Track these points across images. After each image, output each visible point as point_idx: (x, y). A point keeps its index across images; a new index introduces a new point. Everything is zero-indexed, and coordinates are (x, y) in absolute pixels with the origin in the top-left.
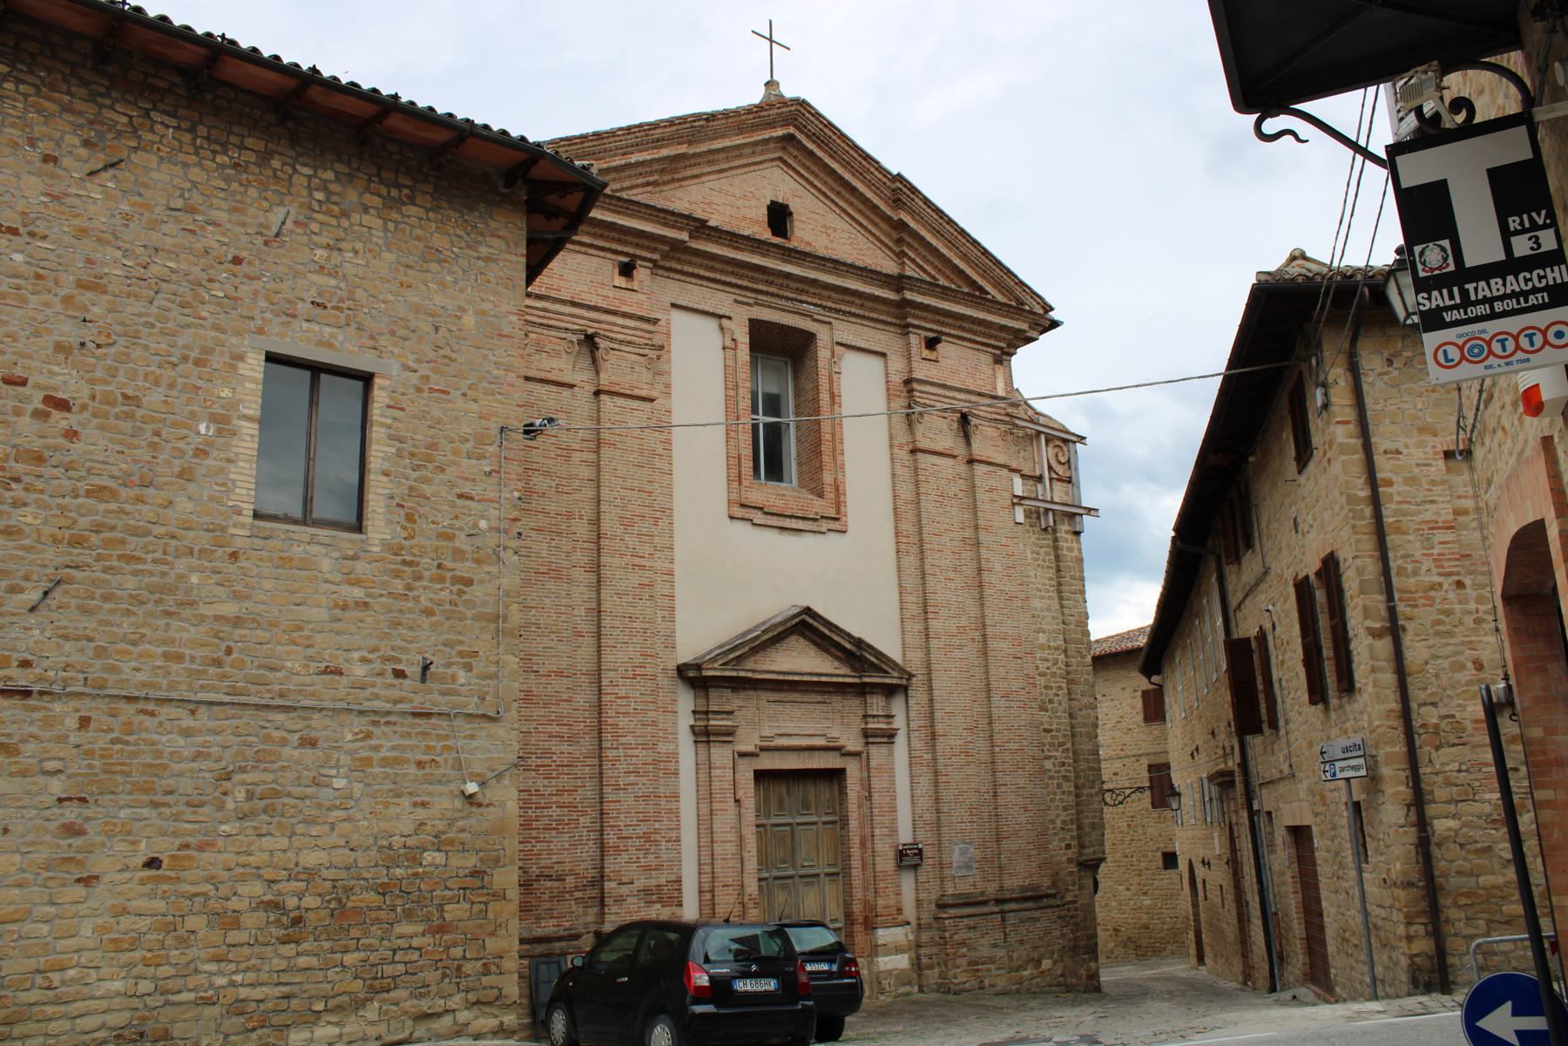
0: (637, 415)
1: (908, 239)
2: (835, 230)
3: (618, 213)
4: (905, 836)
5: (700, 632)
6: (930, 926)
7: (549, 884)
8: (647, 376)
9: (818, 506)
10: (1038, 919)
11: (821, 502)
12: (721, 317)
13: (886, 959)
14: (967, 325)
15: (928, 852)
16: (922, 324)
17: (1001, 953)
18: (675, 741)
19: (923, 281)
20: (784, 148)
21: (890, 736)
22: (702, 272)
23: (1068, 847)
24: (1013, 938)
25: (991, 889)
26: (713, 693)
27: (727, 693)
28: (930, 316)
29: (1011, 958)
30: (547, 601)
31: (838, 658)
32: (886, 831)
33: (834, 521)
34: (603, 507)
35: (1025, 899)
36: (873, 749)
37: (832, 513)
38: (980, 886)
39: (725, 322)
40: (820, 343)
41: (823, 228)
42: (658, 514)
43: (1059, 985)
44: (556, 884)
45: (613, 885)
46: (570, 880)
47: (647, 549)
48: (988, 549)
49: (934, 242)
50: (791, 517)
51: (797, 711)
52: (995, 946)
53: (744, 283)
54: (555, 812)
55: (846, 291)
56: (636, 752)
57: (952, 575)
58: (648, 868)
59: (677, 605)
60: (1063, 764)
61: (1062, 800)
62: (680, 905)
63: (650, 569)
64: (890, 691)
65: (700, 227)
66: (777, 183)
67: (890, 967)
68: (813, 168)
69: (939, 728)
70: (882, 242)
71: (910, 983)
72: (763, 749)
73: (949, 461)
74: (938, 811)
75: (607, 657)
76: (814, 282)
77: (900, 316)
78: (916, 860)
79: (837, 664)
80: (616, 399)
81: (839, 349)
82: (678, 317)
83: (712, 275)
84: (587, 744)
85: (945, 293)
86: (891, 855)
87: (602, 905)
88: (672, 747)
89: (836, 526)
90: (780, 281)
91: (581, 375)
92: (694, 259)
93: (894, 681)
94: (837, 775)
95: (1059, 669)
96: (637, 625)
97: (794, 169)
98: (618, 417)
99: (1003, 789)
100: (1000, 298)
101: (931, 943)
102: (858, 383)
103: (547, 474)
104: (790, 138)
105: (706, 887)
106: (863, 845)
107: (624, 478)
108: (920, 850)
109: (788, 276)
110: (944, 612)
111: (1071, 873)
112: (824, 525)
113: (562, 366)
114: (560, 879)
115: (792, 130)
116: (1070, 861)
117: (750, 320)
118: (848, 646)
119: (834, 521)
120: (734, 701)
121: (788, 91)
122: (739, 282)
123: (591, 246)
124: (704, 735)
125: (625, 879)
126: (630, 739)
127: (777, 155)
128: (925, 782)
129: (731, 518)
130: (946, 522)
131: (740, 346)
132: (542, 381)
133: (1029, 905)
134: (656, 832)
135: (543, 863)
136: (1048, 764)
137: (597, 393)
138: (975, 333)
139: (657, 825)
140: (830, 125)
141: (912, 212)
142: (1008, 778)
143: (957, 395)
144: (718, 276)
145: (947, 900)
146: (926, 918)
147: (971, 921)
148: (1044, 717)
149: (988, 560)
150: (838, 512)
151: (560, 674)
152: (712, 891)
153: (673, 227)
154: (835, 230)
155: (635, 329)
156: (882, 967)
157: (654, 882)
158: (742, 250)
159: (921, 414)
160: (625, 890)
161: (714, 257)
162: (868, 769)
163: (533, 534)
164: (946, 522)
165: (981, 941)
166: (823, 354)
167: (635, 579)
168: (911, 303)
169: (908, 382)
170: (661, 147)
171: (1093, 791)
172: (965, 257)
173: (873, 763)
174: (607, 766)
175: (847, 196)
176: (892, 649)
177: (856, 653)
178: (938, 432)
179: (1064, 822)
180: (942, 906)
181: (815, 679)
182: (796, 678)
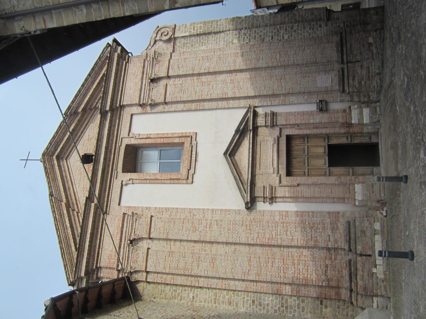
0: (157, 224)
1: (89, 106)
2: (89, 136)
3: (87, 232)
4: (313, 108)
5: (235, 201)
6: (352, 96)
7: (329, 271)
8: (143, 219)
9: (187, 145)
10: (351, 45)
11: (186, 144)
12: (122, 185)
13: (365, 120)
14: (118, 80)
15: (321, 98)
16: (119, 100)
17: (365, 64)
18: (275, 211)
19: (102, 103)
20: (62, 158)
21: (273, 114)
22: (107, 193)
23: (320, 26)
24: (358, 58)
25: (337, 66)
26: (257, 194)
27: (256, 188)
28: (115, 97)
29: (368, 58)
30: (223, 264)
31: (243, 138)
32: (311, 117)
33: (192, 137)
34: (190, 239)
35: (342, 50)
36: (278, 123)
37: (189, 139)
38: (336, 72)
39: (124, 183)
40: (129, 143)
41: (87, 144)
42: (192, 214)
43: (380, 34)
44: (329, 268)
45: (330, 244)
46: (328, 262)
47: (204, 222)
48: (201, 69)
49: (88, 96)
50: (191, 157)
51: (263, 157)
52: (362, 67)
53: (109, 176)
54: (301, 267)
55: (109, 134)
56: (279, 230)
57: (211, 86)
58: (324, 228)
59: (224, 208)
60: (286, 29)
61: (301, 30)
62: (338, 213)
63: (211, 220)
64: (255, 114)
65: (89, 199)
66: (74, 161)
67: (368, 118)
68: (68, 146)
69: (270, 93)
70: (92, 116)
71: (375, 108)
72: (278, 173)
73: (168, 87)
74: (304, 93)
75: (243, 241)
76: (107, 148)
77: (117, 109)
78: (324, 103)
79: (246, 138)
80: (152, 231)
81: (130, 136)
82: (122, 204)
83: (107, 189)
84: (275, 250)
85: (105, 93)
86: (321, 115)
87: (337, 248)
88: (277, 213)
89: (194, 137)
90: (107, 161)
91: (144, 245)
92: (102, 197)
93: (252, 115)
94: (289, 138)
95: (247, 32)
96: (231, 227)
97: (69, 153)
98: (158, 231)
99: (295, 61)
100: (105, 69)
101: (359, 96)
102: (142, 126)
103: (178, 261)
104: (58, 158)
105: (332, 200)
106: (317, 128)
107: (179, 229)
108: (320, 101)
109: (105, 159)
110: (225, 90)
111: (332, 24)
112: (194, 142)
113: (141, 252)
114: (327, 266)
115: (54, 157)
116: (326, 25)
117: (123, 172)
118: (237, 137)
119: (192, 137)
120: (259, 184)
121: (40, 157)
122: (109, 178)
123: (100, 239)
124: (272, 199)
125: (328, 239)
126: (274, 233)
127: (65, 161)
128: (292, 99)
129: (192, 182)
130: (193, 88)
131: (132, 177)
132: (147, 262)
133: (345, 49)
134: (309, 224)
135: (320, 273)
136: (286, 37)
137: (150, 238)
138: (121, 76)
139: (307, 223)
140: (50, 143)
141: (78, 108)
142: (291, 59)
143: (144, 83)
144: (108, 187)
145: (341, 90)
146: (348, 98)
147: (351, 78)
148: (267, 39)
149: (205, 69)
150: (189, 137)
151: (250, 261)
152: (334, 198)
153: (90, 210)
154: (89, 136)
155: (127, 222)
156: (368, 122)
157: (329, 226)
158: (97, 179)
159: (151, 100)
160: (332, 239)
161: (100, 190)
162: (286, 125)
163: (200, 268)
164: (193, 88)
165: (359, 73)
166: (133, 142)
167: (215, 227)
168: (111, 106)
169: (140, 105)
170: (63, 213)
171: (297, 15)
172: (93, 83)
173: (284, 123)
174: (284, 244)
175: (76, 132)
176: (241, 113)
177: (241, 133)
178: (157, 93)
179: (310, 29)
180: (344, 91)
181: (251, 151)
182: (251, 159)
